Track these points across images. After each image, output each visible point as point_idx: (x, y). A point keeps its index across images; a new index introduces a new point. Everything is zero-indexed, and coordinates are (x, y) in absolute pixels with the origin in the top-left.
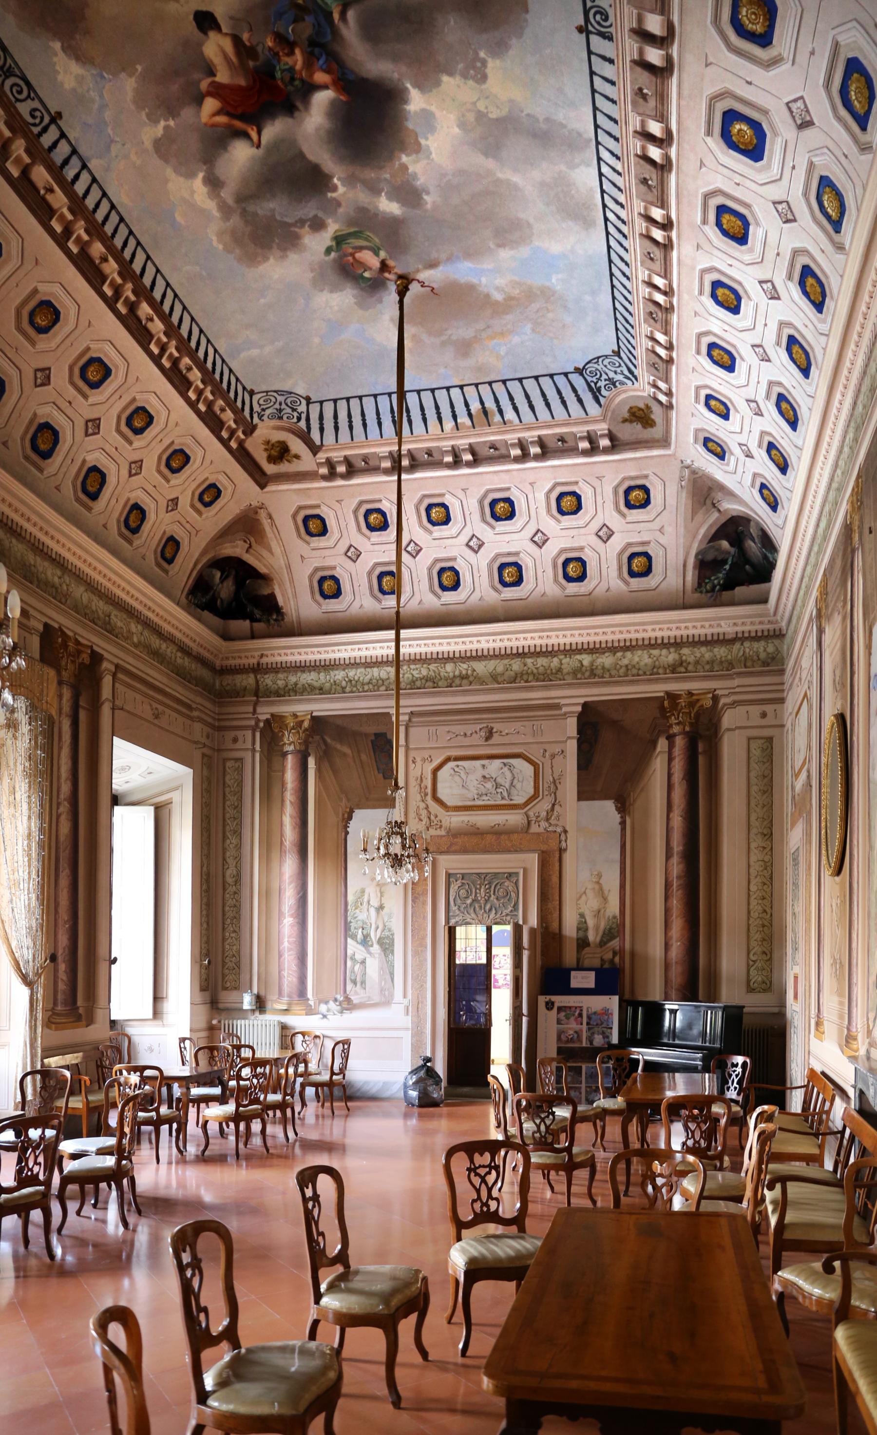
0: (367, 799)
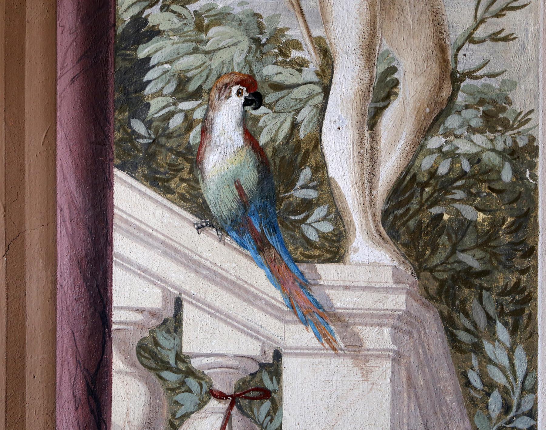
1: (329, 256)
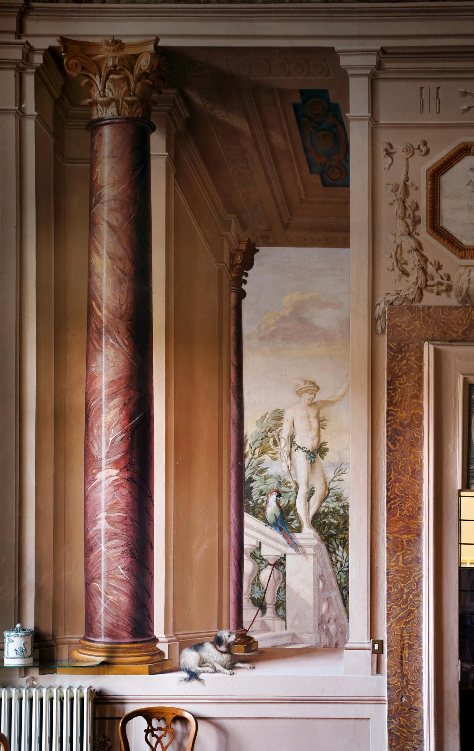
0: (286, 226)
1: (297, 531)
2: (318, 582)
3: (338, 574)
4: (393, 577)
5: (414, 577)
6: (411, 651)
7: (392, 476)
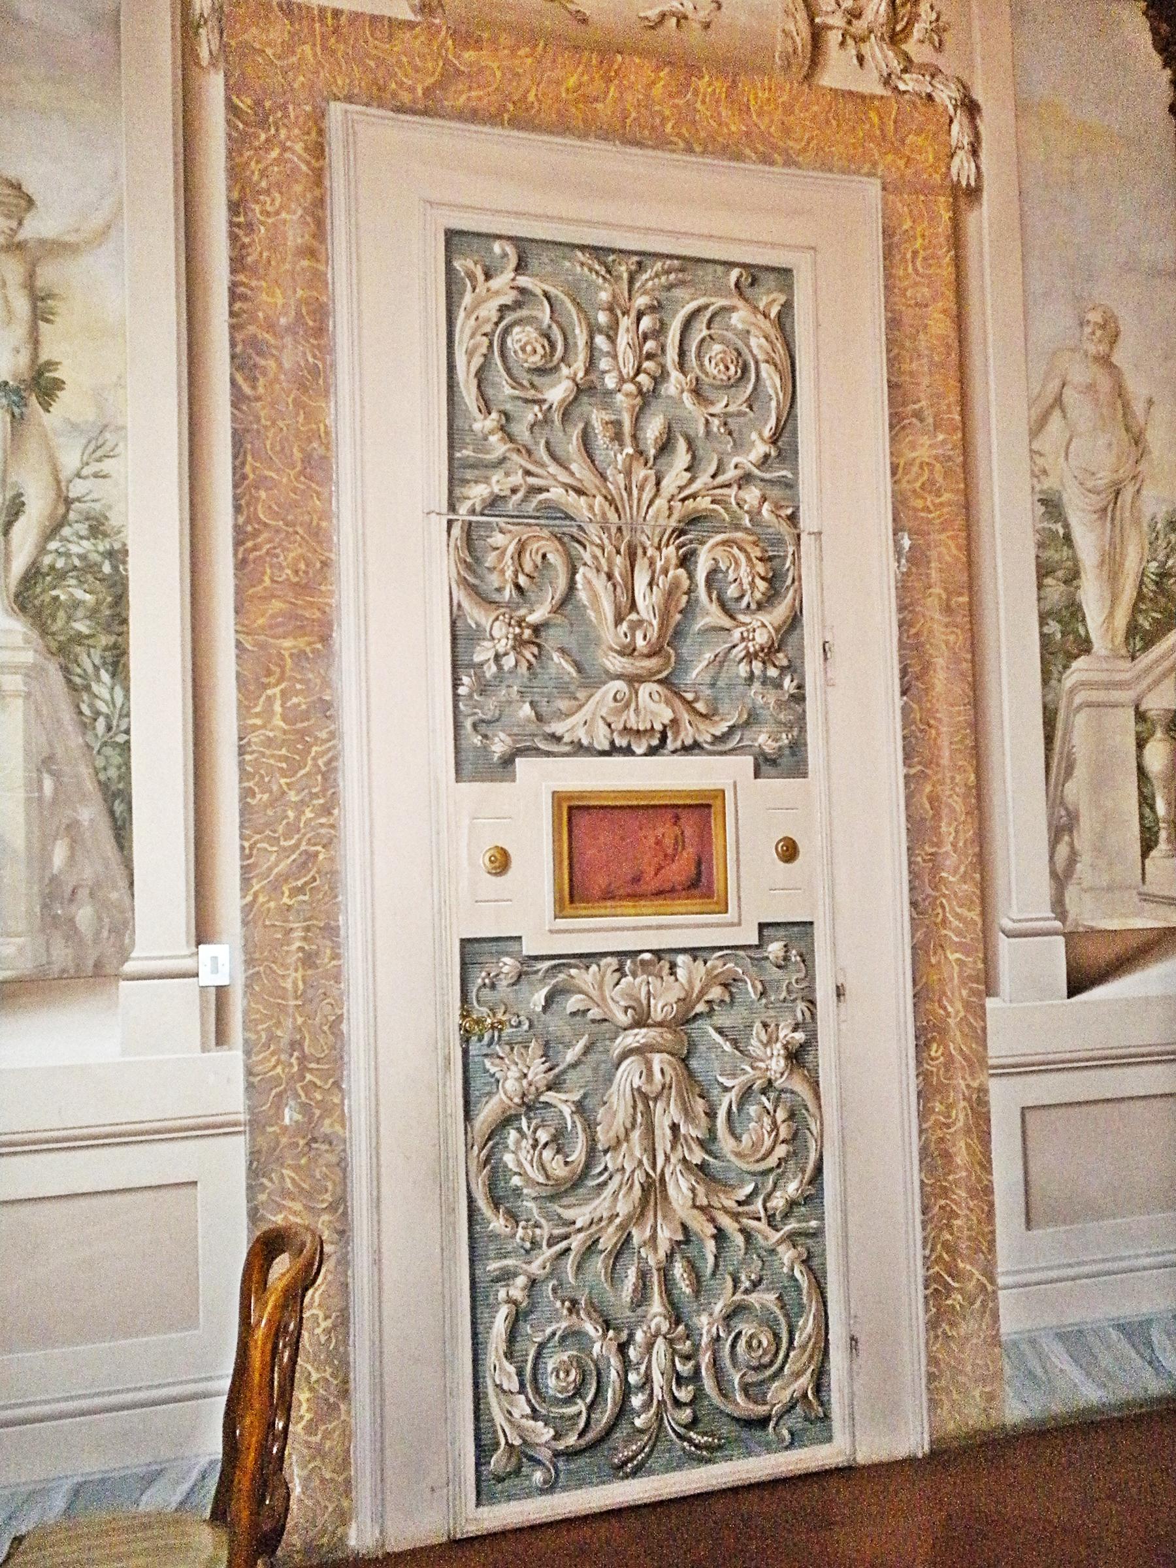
2: (40, 782)
3: (99, 752)
4: (256, 759)
5: (314, 759)
6: (310, 972)
7: (247, 469)
